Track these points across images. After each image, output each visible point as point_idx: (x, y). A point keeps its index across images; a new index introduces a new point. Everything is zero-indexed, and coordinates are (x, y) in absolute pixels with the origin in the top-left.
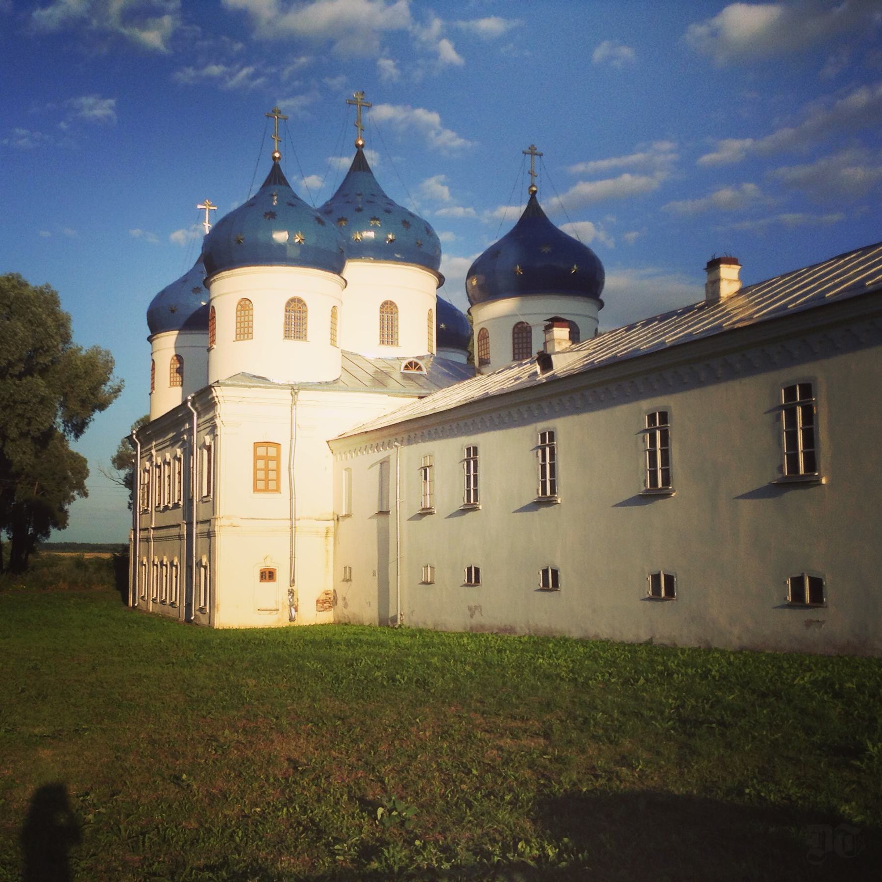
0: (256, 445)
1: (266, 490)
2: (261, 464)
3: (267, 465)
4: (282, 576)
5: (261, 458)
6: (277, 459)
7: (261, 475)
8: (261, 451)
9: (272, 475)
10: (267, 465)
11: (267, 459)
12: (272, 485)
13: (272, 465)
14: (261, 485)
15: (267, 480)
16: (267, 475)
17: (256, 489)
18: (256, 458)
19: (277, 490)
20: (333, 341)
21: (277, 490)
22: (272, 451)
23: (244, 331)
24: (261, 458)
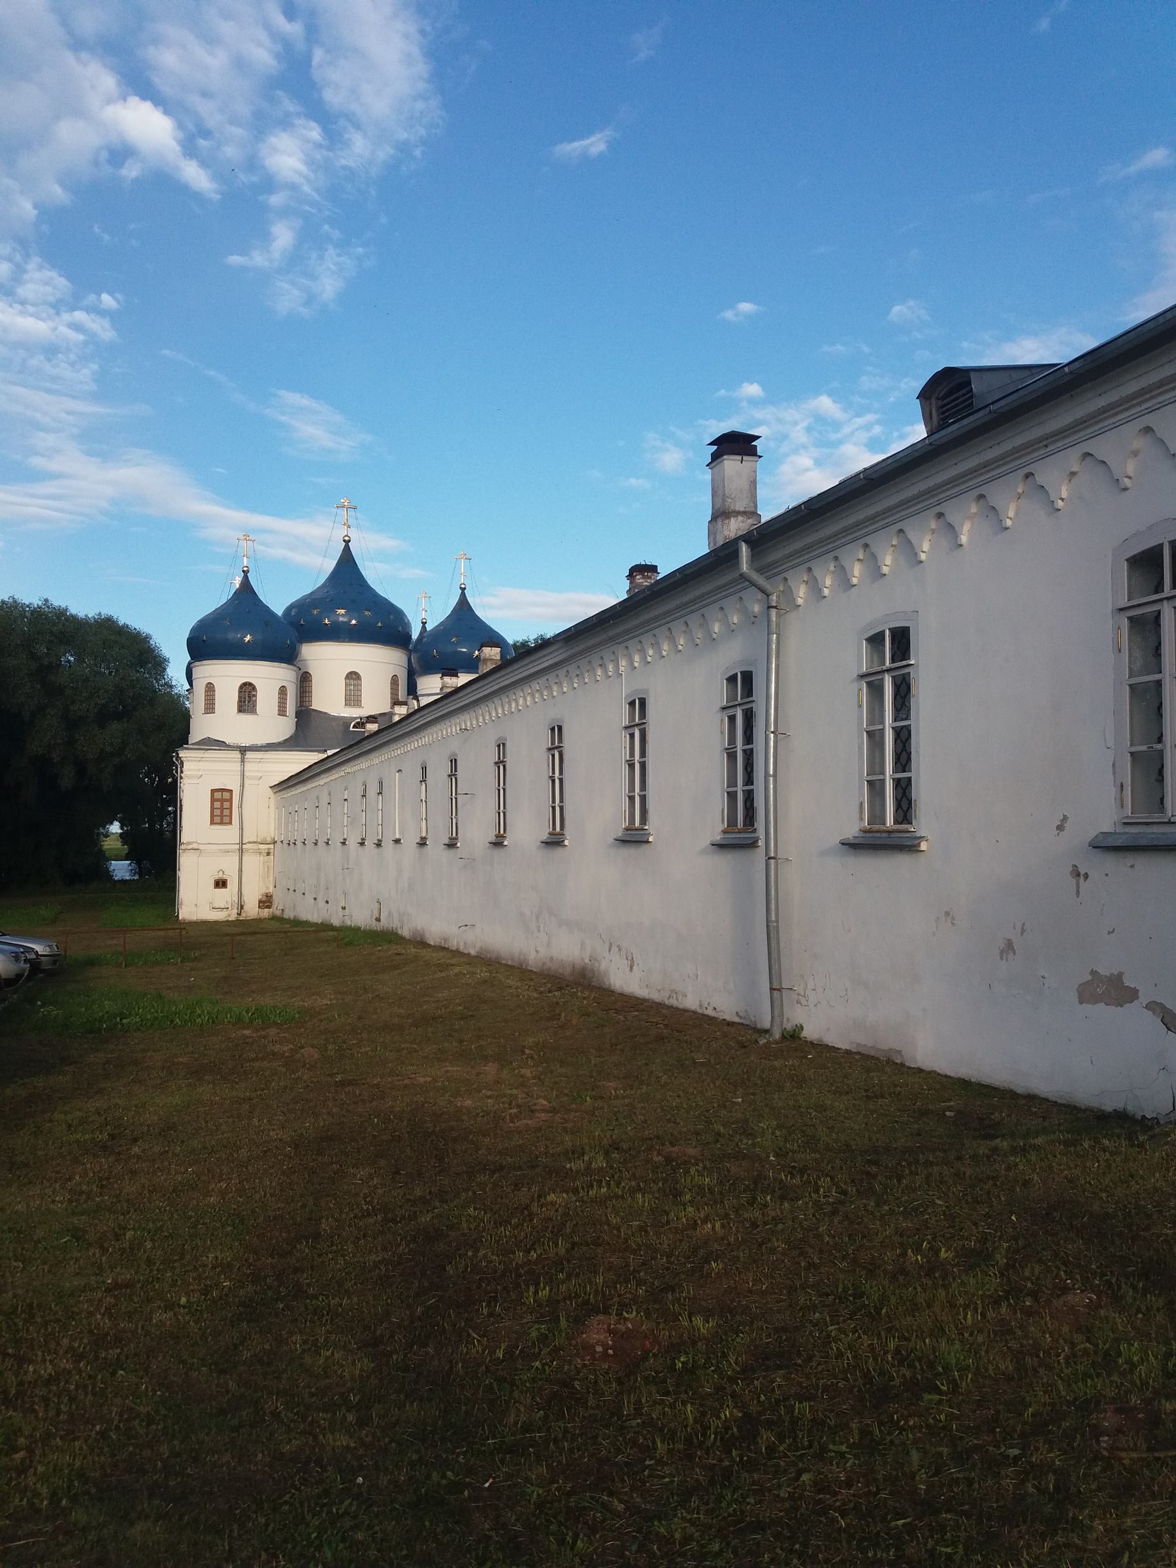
0: (213, 791)
1: (222, 823)
2: (217, 804)
3: (222, 805)
4: (233, 885)
5: (218, 800)
6: (230, 800)
7: (217, 812)
8: (218, 795)
9: (226, 812)
10: (222, 805)
11: (222, 801)
12: (226, 819)
13: (226, 805)
14: (217, 819)
15: (222, 816)
16: (222, 812)
17: (212, 823)
18: (213, 800)
19: (230, 823)
20: (282, 712)
21: (230, 823)
22: (226, 795)
23: (210, 708)
24: (218, 800)
